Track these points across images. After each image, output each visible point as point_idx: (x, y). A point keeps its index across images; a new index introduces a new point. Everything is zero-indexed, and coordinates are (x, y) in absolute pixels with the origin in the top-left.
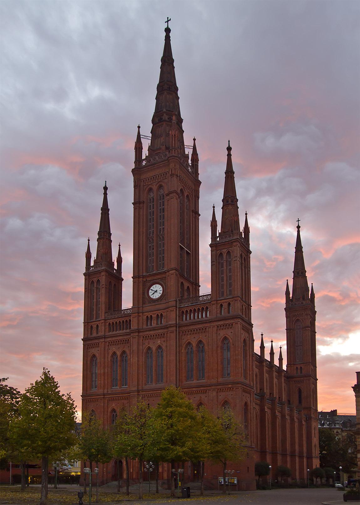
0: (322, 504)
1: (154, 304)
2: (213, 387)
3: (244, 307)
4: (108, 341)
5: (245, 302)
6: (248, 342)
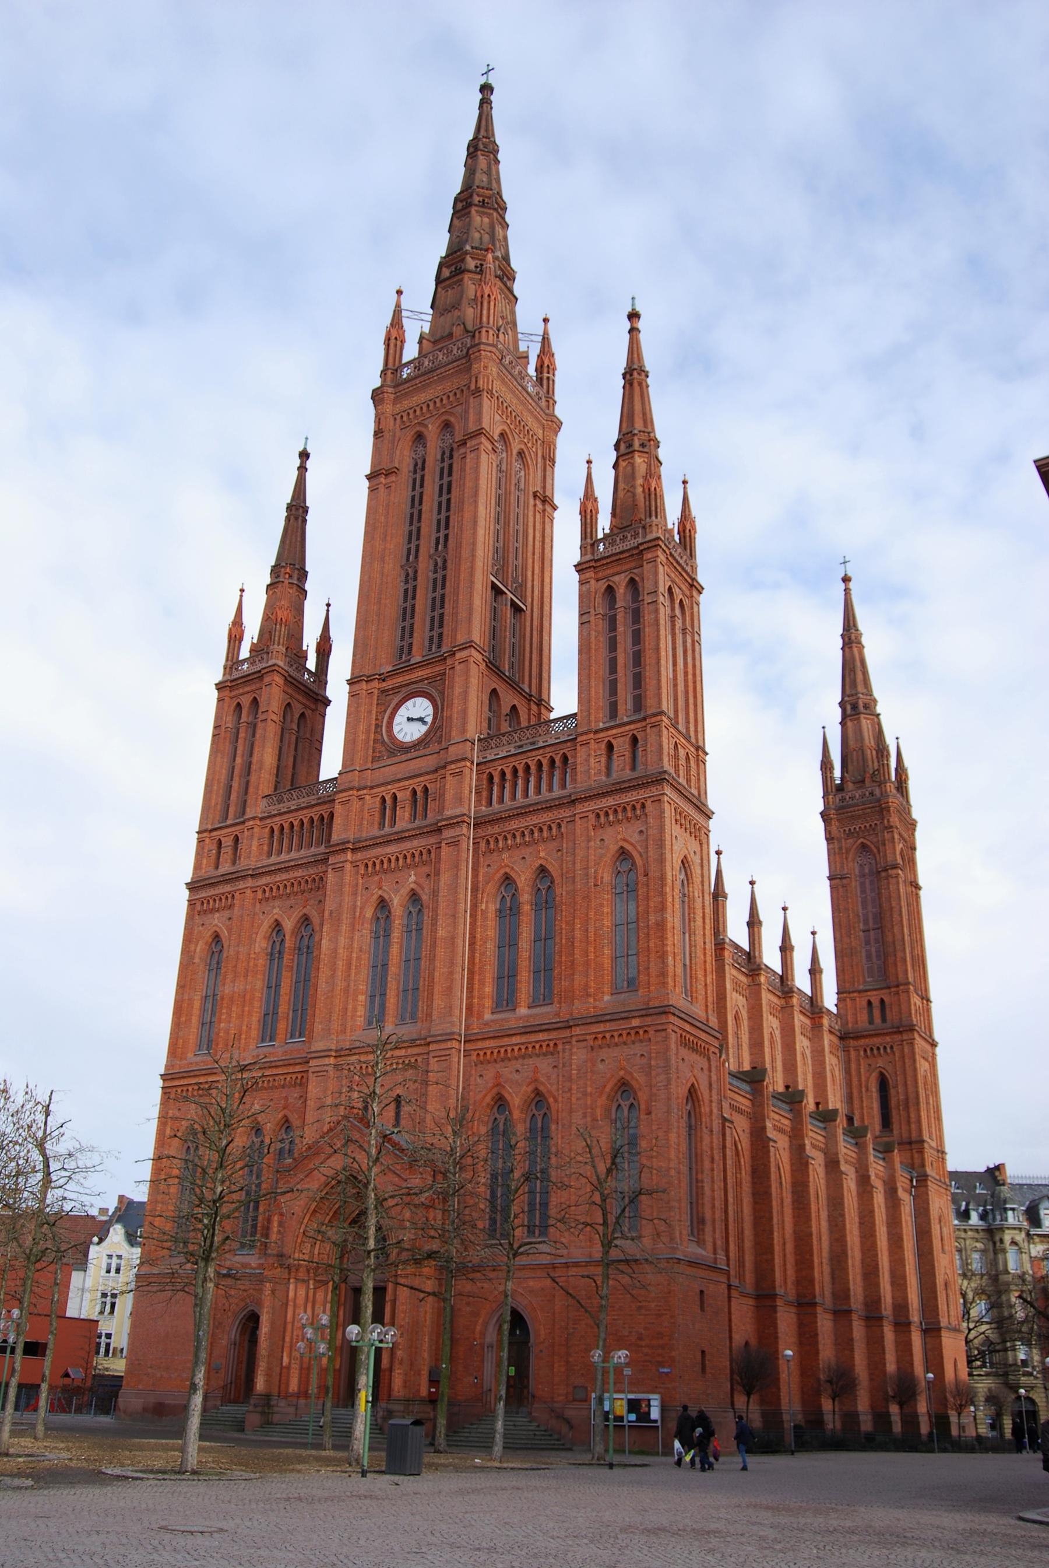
0: (1021, 1519)
1: (404, 757)
2: (577, 1031)
3: (681, 750)
4: (260, 886)
5: (685, 738)
6: (699, 871)
